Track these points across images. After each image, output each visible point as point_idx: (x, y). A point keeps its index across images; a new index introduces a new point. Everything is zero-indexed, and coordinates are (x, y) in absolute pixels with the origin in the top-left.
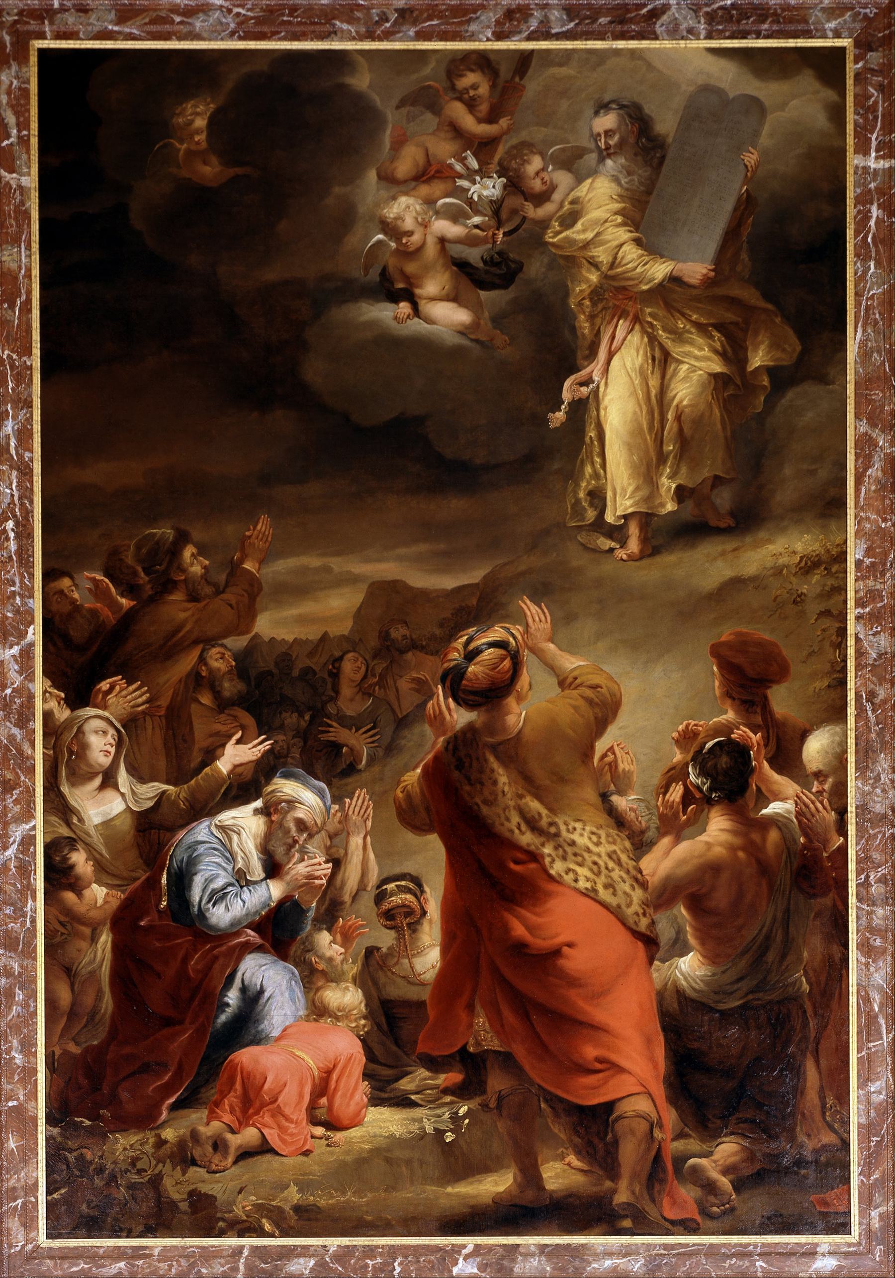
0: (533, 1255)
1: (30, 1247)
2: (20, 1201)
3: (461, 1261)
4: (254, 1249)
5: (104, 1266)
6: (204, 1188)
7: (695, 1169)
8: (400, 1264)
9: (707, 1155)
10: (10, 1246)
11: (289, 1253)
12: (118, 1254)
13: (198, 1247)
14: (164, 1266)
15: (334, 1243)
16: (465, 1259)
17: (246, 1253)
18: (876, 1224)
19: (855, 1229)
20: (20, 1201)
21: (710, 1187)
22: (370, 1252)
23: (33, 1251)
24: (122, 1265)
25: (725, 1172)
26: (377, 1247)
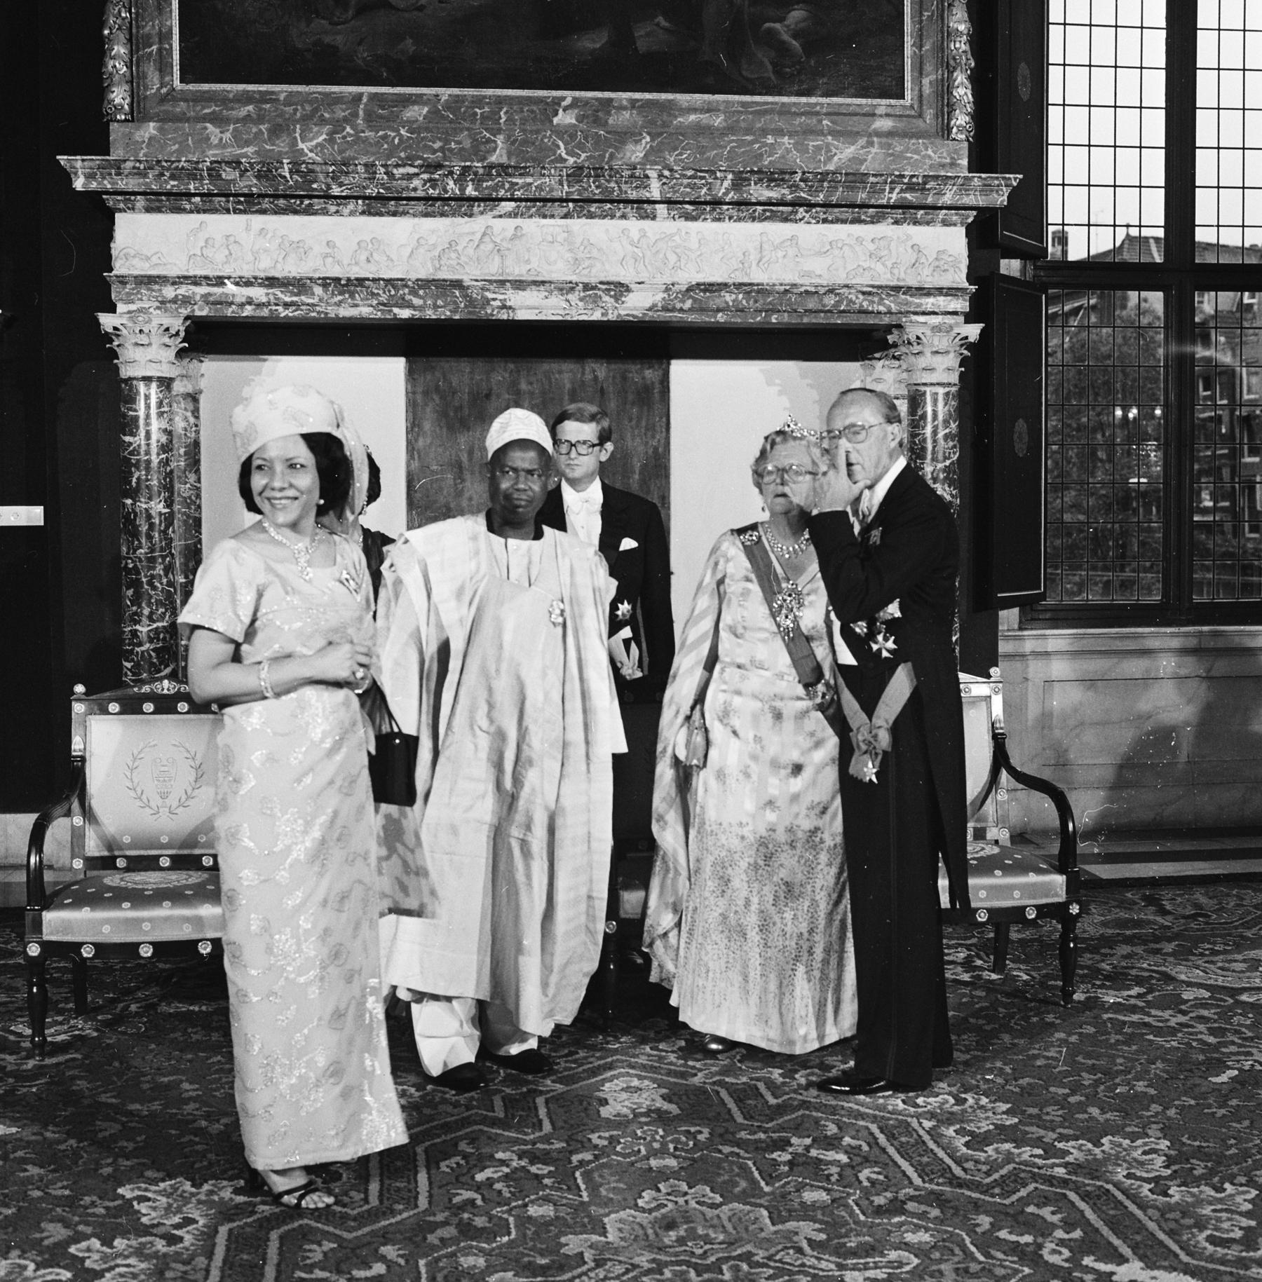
0: (625, 108)
1: (164, 90)
2: (155, 47)
3: (561, 111)
4: (373, 97)
5: (232, 109)
6: (327, 39)
7: (770, 32)
9: (781, 20)
10: (146, 88)
11: (407, 101)
12: (247, 98)
13: (319, 93)
14: (289, 109)
15: (445, 93)
18: (927, 90)
20: (155, 47)
21: (782, 49)
22: (479, 101)
23: (168, 94)
24: (250, 108)
25: (795, 36)
26: (485, 97)
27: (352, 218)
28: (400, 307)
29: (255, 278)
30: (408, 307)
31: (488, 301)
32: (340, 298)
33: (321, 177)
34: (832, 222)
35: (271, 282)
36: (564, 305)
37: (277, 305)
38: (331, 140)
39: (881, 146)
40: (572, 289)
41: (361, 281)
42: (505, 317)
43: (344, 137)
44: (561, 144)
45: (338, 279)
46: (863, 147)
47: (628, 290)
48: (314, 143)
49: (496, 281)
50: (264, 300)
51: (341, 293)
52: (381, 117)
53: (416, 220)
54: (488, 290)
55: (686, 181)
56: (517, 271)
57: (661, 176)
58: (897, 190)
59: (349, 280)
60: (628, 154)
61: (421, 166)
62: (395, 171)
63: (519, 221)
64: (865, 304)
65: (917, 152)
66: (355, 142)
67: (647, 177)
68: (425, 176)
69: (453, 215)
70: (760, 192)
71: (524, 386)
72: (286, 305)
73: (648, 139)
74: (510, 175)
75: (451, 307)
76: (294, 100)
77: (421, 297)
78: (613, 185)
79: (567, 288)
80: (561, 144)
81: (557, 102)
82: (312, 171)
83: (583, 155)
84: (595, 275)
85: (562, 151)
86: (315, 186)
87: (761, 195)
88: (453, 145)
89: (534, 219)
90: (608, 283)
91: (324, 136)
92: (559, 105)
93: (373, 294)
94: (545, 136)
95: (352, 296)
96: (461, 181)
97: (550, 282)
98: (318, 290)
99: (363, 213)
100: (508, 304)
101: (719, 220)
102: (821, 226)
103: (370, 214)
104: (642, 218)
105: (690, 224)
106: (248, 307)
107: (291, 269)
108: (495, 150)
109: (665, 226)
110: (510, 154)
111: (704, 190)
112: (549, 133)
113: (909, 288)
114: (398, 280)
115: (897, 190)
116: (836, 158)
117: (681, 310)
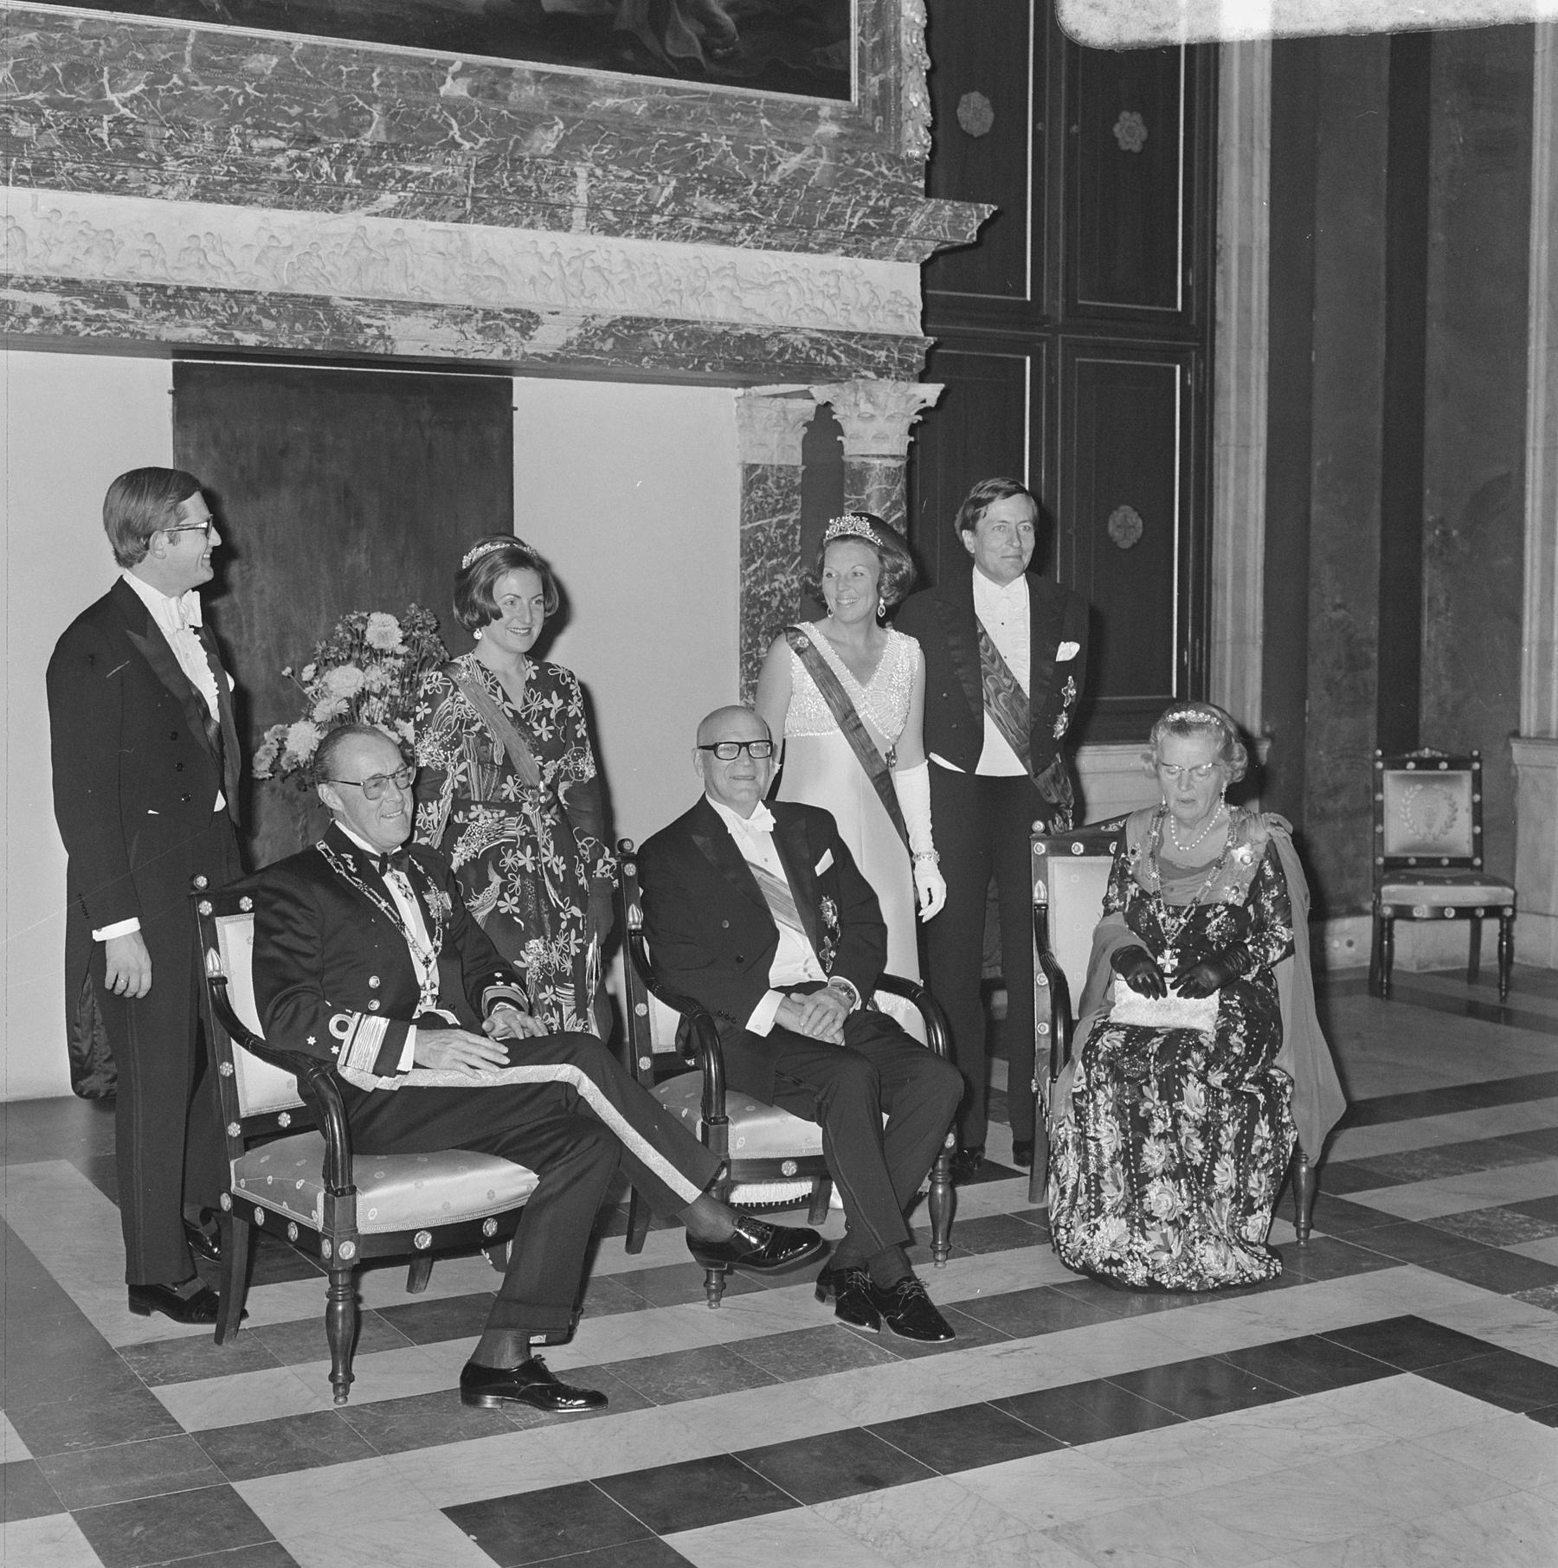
0: (528, 83)
3: (449, 79)
4: (203, 35)
8: (380, 75)
11: (248, 46)
13: (130, 25)
14: (88, 44)
15: (299, 40)
16: (454, 78)
17: (191, 39)
19: (855, 95)
24: (33, 35)
26: (351, 51)
27: (178, 204)
28: (244, 331)
29: (47, 279)
30: (254, 330)
31: (361, 328)
32: (164, 313)
33: (152, 144)
34: (775, 249)
35: (70, 286)
36: (457, 336)
37: (75, 319)
38: (151, 93)
39: (830, 158)
40: (469, 316)
41: (194, 291)
42: (381, 350)
43: (170, 90)
44: (453, 122)
45: (164, 288)
46: (810, 157)
47: (538, 322)
48: (128, 94)
49: (374, 301)
50: (58, 311)
51: (166, 306)
52: (215, 65)
53: (265, 212)
54: (361, 313)
55: (620, 185)
56: (399, 288)
57: (591, 175)
58: (859, 214)
59: (179, 289)
60: (537, 144)
61: (290, 140)
62: (254, 143)
63: (399, 222)
64: (812, 353)
65: (869, 167)
66: (184, 97)
67: (574, 175)
68: (293, 153)
69: (315, 208)
70: (706, 204)
71: (329, 439)
72: (89, 321)
73: (561, 126)
74: (402, 160)
75: (312, 334)
76: (94, 31)
77: (272, 318)
78: (530, 183)
79: (460, 316)
80: (453, 122)
81: (444, 65)
82: (141, 135)
83: (482, 140)
84: (493, 298)
85: (455, 132)
86: (141, 155)
87: (706, 209)
88: (316, 113)
89: (418, 221)
90: (516, 311)
91: (142, 86)
92: (446, 69)
93: (208, 310)
94: (434, 111)
95: (181, 313)
96: (338, 163)
97: (442, 306)
98: (134, 301)
99: (195, 197)
100: (387, 333)
101: (645, 237)
102: (762, 252)
103: (204, 199)
104: (554, 228)
105: (610, 239)
106: (34, 321)
107: (92, 269)
108: (370, 125)
109: (580, 242)
110: (389, 130)
111: (640, 198)
112: (438, 107)
113: (863, 335)
114: (245, 292)
115: (859, 214)
116: (780, 168)
117: (600, 352)
